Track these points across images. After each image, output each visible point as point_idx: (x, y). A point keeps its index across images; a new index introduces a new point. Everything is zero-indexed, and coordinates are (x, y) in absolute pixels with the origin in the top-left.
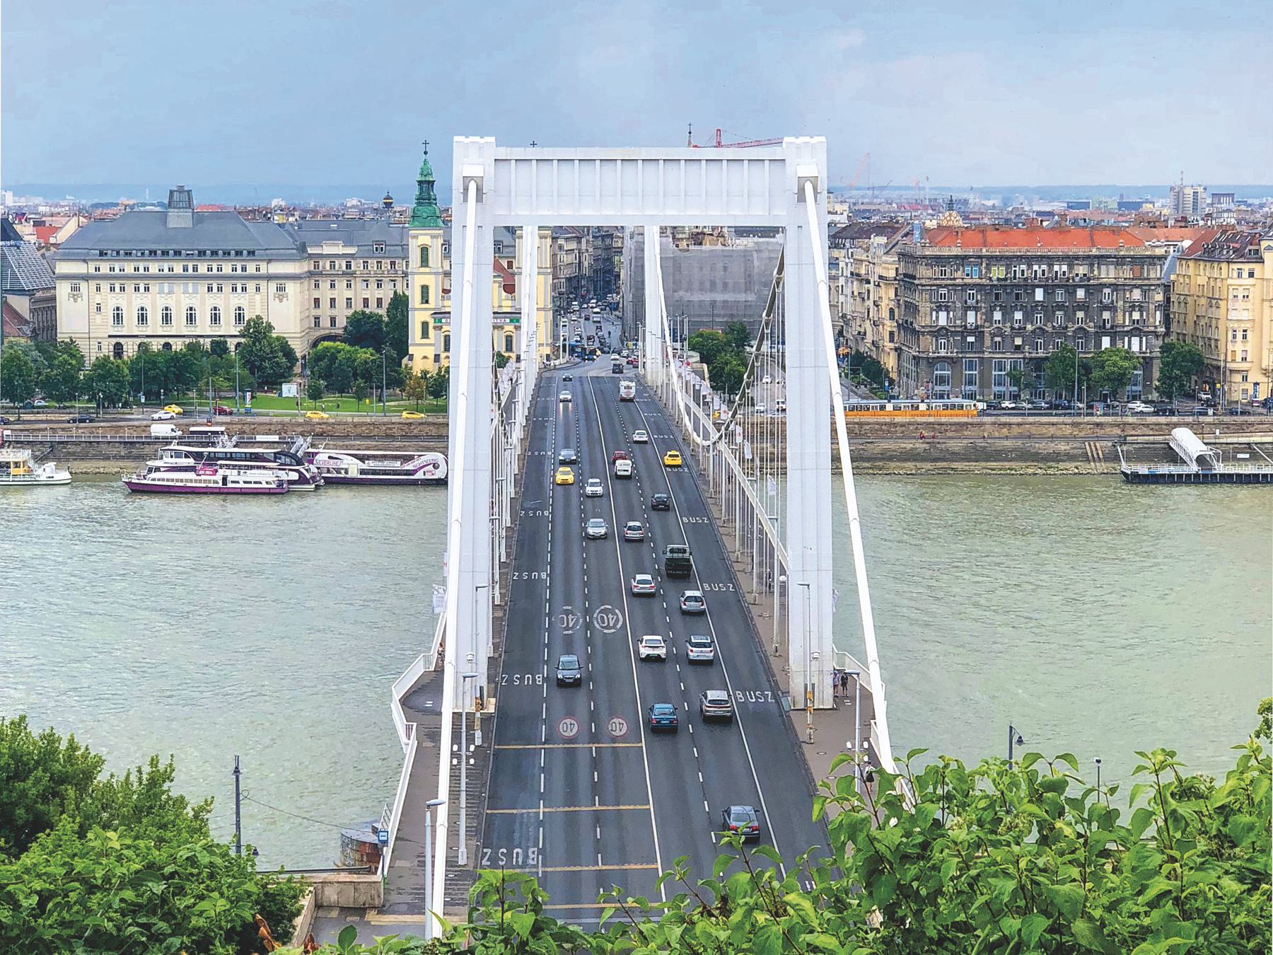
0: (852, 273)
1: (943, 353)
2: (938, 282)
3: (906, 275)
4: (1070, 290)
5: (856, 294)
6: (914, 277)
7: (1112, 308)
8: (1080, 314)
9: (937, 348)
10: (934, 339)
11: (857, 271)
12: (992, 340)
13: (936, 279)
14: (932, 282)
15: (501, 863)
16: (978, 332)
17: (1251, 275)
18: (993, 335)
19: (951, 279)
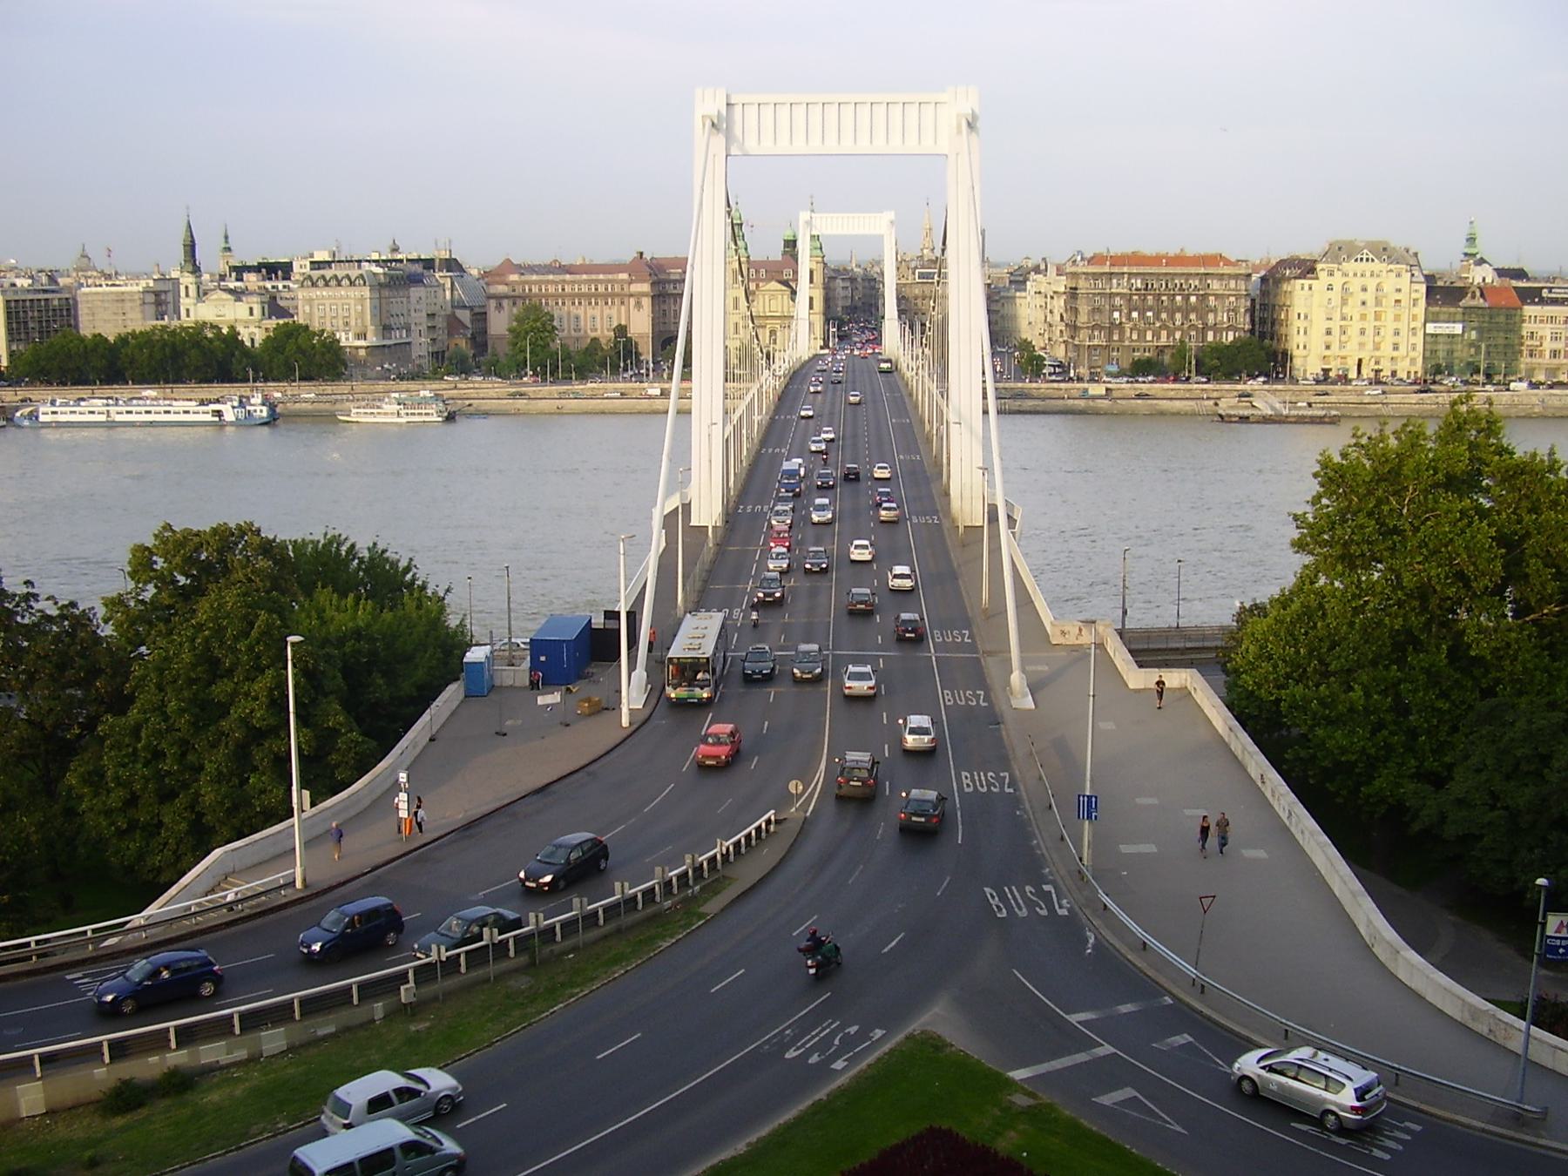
1: (1096, 342)
3: (1071, 288)
7: (1214, 310)
17: (1310, 288)
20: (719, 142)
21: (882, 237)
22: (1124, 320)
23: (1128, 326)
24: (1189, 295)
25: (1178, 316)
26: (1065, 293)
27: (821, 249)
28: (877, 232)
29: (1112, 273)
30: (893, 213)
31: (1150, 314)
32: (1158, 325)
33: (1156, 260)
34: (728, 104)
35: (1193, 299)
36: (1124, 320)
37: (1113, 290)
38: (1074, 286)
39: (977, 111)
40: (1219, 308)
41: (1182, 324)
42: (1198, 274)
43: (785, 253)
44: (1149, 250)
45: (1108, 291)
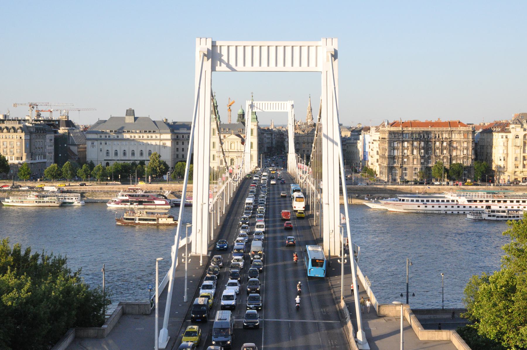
2: (393, 140)
3: (382, 138)
7: (456, 148)
9: (393, 163)
13: (393, 139)
14: (391, 140)
19: (398, 139)
20: (208, 64)
21: (287, 113)
23: (411, 157)
24: (443, 142)
27: (257, 118)
28: (285, 111)
29: (404, 131)
30: (293, 101)
33: (426, 124)
34: (212, 46)
35: (445, 144)
38: (384, 137)
39: (337, 49)
42: (447, 131)
43: (238, 121)
44: (423, 121)
45: (401, 139)
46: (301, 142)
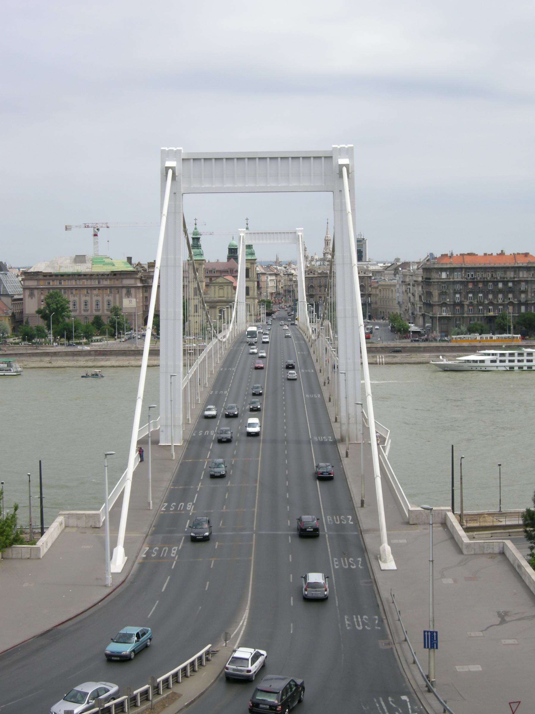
0: (402, 282)
1: (444, 314)
3: (426, 279)
4: (505, 283)
5: (404, 291)
6: (430, 279)
7: (525, 292)
8: (510, 296)
10: (440, 308)
11: (405, 280)
12: (468, 308)
15: (171, 509)
16: (461, 305)
18: (468, 306)
22: (463, 299)
25: (500, 296)
26: (422, 282)
31: (481, 295)
32: (486, 302)
36: (463, 299)
37: (456, 280)
38: (428, 277)
40: (529, 290)
41: (504, 301)
45: (451, 280)
46: (316, 285)
